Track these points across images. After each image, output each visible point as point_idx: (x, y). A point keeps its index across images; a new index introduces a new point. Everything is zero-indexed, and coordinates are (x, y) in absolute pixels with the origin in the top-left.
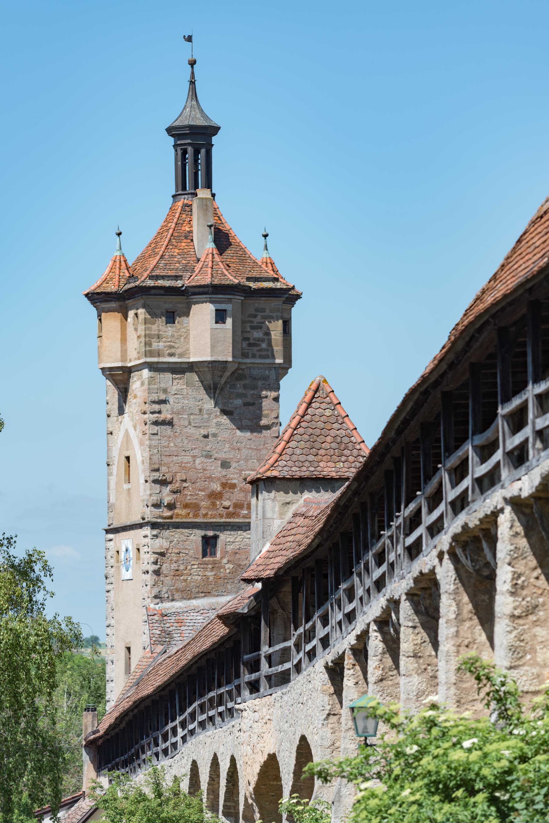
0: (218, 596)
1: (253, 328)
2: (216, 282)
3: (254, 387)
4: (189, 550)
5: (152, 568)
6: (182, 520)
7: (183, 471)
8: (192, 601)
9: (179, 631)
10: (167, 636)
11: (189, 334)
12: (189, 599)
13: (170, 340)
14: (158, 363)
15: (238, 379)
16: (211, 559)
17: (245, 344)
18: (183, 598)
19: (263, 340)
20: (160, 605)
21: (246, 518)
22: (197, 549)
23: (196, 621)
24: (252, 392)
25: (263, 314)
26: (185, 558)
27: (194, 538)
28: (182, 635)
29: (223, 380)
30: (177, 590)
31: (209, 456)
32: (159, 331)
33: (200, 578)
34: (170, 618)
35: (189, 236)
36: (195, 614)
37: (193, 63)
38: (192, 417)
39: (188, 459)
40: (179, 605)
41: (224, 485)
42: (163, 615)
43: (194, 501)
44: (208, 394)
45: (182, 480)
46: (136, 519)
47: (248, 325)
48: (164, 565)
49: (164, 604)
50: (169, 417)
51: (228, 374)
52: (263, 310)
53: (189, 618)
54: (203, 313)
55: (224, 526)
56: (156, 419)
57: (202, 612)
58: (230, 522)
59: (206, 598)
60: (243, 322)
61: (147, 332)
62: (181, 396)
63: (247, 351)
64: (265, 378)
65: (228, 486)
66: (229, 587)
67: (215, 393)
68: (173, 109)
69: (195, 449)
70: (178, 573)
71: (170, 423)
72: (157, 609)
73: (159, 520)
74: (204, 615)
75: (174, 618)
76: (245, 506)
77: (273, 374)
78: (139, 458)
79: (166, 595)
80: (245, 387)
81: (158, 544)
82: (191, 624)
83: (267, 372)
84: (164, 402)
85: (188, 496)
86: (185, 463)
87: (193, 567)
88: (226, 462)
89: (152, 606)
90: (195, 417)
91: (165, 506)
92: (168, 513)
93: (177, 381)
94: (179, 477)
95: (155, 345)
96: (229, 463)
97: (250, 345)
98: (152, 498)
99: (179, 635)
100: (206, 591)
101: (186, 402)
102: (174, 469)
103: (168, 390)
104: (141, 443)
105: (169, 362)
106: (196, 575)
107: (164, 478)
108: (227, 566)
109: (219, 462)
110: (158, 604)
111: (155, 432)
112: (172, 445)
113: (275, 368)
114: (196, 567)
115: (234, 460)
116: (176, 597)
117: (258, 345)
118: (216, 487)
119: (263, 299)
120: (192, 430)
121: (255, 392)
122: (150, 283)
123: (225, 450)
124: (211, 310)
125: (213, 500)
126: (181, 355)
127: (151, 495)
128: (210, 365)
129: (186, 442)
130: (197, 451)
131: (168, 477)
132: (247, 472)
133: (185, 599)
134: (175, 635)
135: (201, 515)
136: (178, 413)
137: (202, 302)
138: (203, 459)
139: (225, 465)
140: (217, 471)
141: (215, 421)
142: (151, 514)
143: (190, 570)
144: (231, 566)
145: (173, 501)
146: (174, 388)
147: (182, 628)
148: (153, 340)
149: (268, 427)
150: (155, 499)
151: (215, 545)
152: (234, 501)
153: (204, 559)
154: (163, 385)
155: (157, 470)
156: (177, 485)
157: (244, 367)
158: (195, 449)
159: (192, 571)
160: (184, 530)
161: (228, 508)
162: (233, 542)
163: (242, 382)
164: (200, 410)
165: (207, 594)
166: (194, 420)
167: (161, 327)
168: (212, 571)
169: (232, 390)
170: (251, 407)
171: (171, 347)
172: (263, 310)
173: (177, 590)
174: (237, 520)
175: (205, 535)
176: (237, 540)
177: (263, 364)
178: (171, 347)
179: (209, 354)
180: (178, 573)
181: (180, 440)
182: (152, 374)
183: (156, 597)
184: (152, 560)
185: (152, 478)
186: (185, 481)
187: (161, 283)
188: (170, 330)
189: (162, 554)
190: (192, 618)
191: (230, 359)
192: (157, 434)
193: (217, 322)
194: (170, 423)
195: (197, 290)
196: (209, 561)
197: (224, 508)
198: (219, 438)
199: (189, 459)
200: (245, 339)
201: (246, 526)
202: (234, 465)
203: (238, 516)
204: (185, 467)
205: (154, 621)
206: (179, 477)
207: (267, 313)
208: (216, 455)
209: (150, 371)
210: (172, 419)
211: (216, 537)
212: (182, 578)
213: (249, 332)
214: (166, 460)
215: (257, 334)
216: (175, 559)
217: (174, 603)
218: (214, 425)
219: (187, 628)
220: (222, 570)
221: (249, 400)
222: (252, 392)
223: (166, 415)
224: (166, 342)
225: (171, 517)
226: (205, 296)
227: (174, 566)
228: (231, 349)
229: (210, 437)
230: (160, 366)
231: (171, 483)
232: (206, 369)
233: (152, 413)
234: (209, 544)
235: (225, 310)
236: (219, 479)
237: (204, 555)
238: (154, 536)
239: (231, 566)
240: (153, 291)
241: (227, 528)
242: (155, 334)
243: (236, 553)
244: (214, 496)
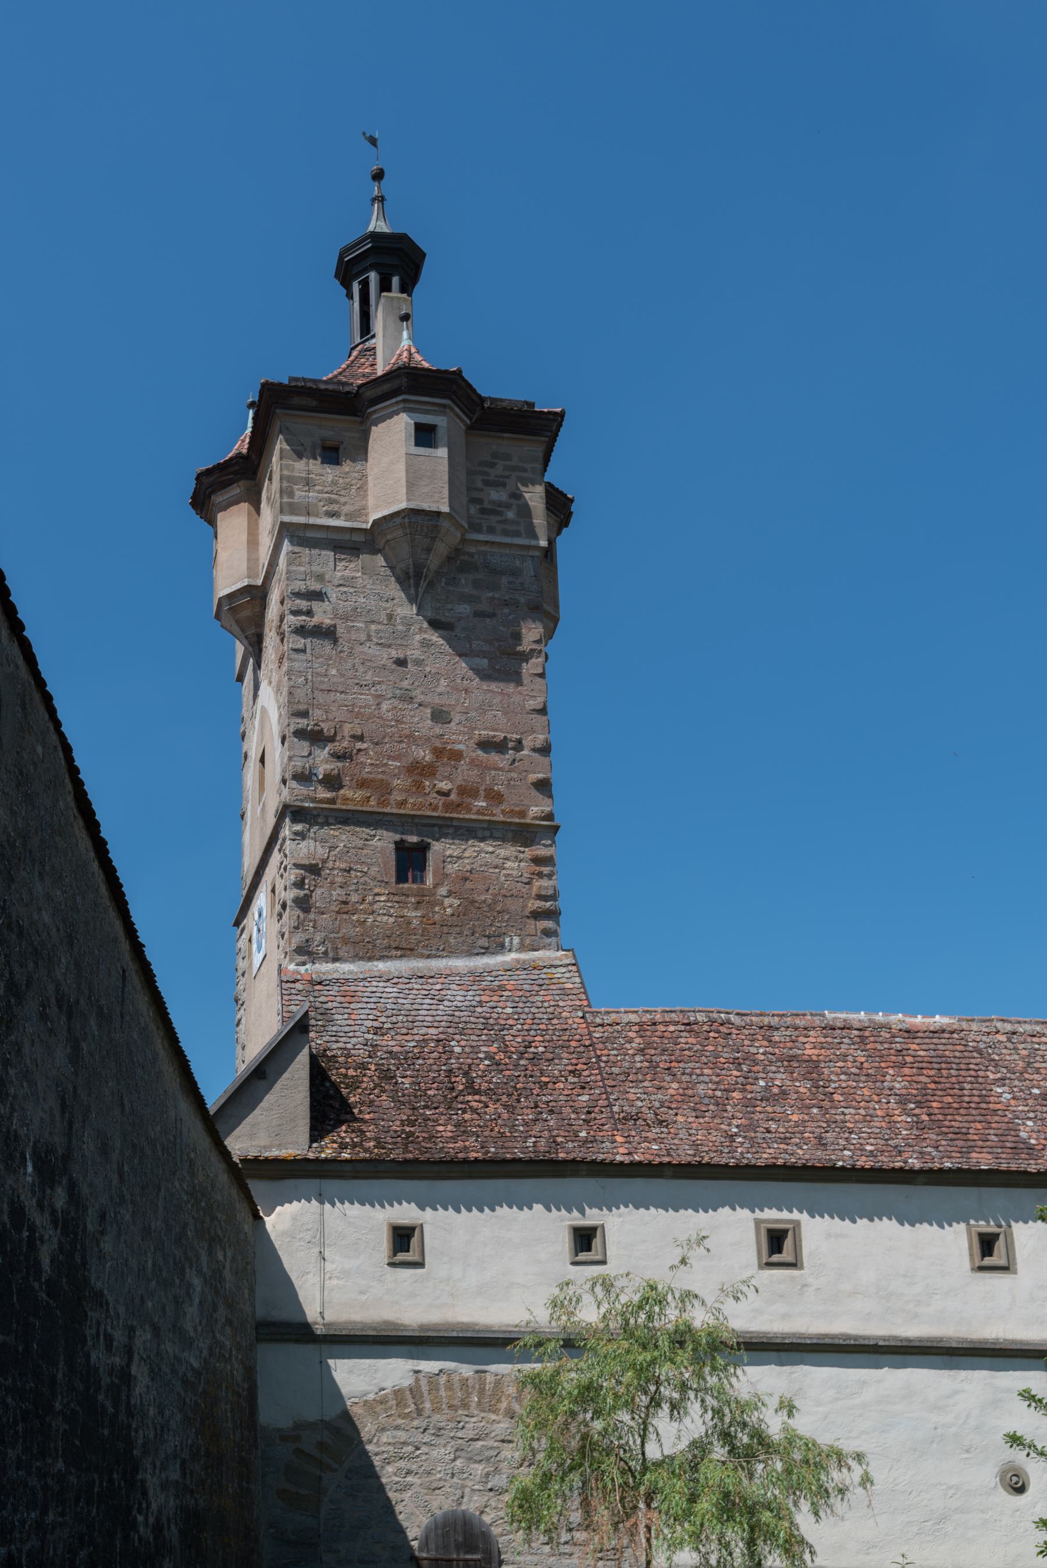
0: (429, 957)
1: (488, 483)
4: (369, 865)
5: (290, 895)
6: (354, 808)
7: (357, 721)
8: (375, 963)
9: (346, 1010)
10: (319, 1017)
11: (366, 483)
12: (370, 959)
13: (329, 489)
14: (306, 526)
16: (415, 886)
17: (473, 510)
18: (357, 957)
19: (508, 506)
20: (308, 966)
21: (483, 814)
22: (385, 864)
23: (384, 995)
24: (491, 595)
25: (507, 463)
26: (362, 880)
27: (379, 843)
28: (353, 1017)
29: (434, 562)
30: (346, 941)
31: (407, 698)
32: (309, 472)
33: (392, 920)
34: (327, 988)
36: (382, 984)
38: (373, 627)
39: (366, 698)
40: (346, 968)
41: (438, 752)
42: (313, 983)
43: (380, 776)
44: (403, 590)
45: (353, 737)
48: (319, 891)
49: (317, 965)
50: (328, 621)
51: (442, 549)
52: (507, 457)
53: (369, 989)
54: (392, 436)
55: (440, 827)
56: (302, 623)
57: (395, 980)
58: (452, 819)
59: (405, 960)
60: (470, 473)
61: (285, 472)
62: (352, 590)
63: (478, 521)
64: (515, 573)
66: (452, 940)
67: (417, 585)
69: (379, 683)
70: (345, 908)
71: (328, 634)
72: (303, 972)
73: (307, 805)
74: (400, 986)
75: (337, 989)
76: (482, 793)
77: (528, 569)
79: (321, 949)
80: (476, 584)
81: (305, 851)
82: (372, 1000)
83: (518, 563)
84: (318, 596)
85: (367, 763)
86: (361, 707)
87: (377, 898)
88: (441, 711)
89: (292, 967)
90: (380, 627)
91: (320, 782)
92: (323, 794)
93: (343, 563)
94: (347, 730)
95: (300, 494)
96: (448, 713)
97: (483, 511)
98: (292, 763)
99: (346, 1016)
100: (405, 946)
102: (340, 714)
103: (327, 577)
105: (328, 527)
106: (384, 911)
107: (316, 728)
108: (447, 902)
109: (429, 711)
110: (304, 964)
111: (300, 646)
112: (334, 672)
113: (532, 557)
114: (383, 898)
115: (458, 709)
116: (341, 954)
117: (500, 513)
118: (425, 755)
119: (506, 435)
120: (371, 650)
121: (497, 596)
123: (439, 690)
124: (407, 423)
125: (417, 778)
126: (350, 517)
127: (290, 758)
128: (406, 520)
129: (361, 669)
130: (384, 687)
131: (327, 728)
132: (482, 732)
133: (361, 959)
134: (336, 1017)
136: (346, 618)
137: (390, 416)
138: (396, 702)
139: (440, 716)
140: (425, 726)
141: (418, 637)
142: (291, 794)
143: (371, 904)
144: (456, 902)
145: (336, 772)
146: (339, 574)
147: (352, 1006)
149: (525, 657)
150: (299, 763)
151: (422, 867)
152: (459, 783)
153: (401, 886)
155: (304, 714)
156: (345, 744)
157: (472, 549)
158: (379, 683)
159: (375, 906)
160: (358, 829)
161: (446, 794)
162: (459, 858)
164: (390, 617)
165: (406, 951)
166: (377, 632)
167: (311, 467)
168: (416, 909)
169: (451, 588)
170: (488, 620)
171: (331, 502)
172: (507, 457)
174: (467, 817)
175: (402, 841)
176: (466, 854)
177: (510, 545)
178: (331, 502)
179: (405, 497)
180: (345, 908)
181: (349, 665)
182: (297, 549)
183: (300, 950)
184: (292, 877)
185: (292, 729)
186: (361, 738)
188: (330, 473)
189: (314, 870)
190: (375, 989)
191: (445, 509)
192: (304, 651)
193: (417, 444)
194: (328, 634)
196: (409, 889)
197: (439, 793)
198: (428, 669)
200: (473, 500)
201: (483, 829)
203: (469, 810)
204: (359, 713)
205: (293, 991)
206: (347, 730)
208: (421, 698)
209: (291, 542)
210: (335, 626)
211: (423, 848)
212: (355, 918)
213: (482, 490)
214: (321, 698)
215: (497, 495)
216: (339, 879)
217: (337, 965)
219: (360, 1005)
220: (437, 909)
222: (491, 595)
223: (323, 615)
224: (319, 492)
225: (332, 801)
226: (394, 400)
227: (337, 893)
228: (446, 492)
229: (409, 666)
230: (310, 534)
231: (332, 739)
232: (399, 533)
233: (295, 613)
234: (410, 861)
236: (428, 740)
237: (401, 878)
238: (296, 833)
239: (456, 902)
240: (296, 401)
241: (446, 831)
242: (302, 478)
243: (466, 879)
244: (419, 771)
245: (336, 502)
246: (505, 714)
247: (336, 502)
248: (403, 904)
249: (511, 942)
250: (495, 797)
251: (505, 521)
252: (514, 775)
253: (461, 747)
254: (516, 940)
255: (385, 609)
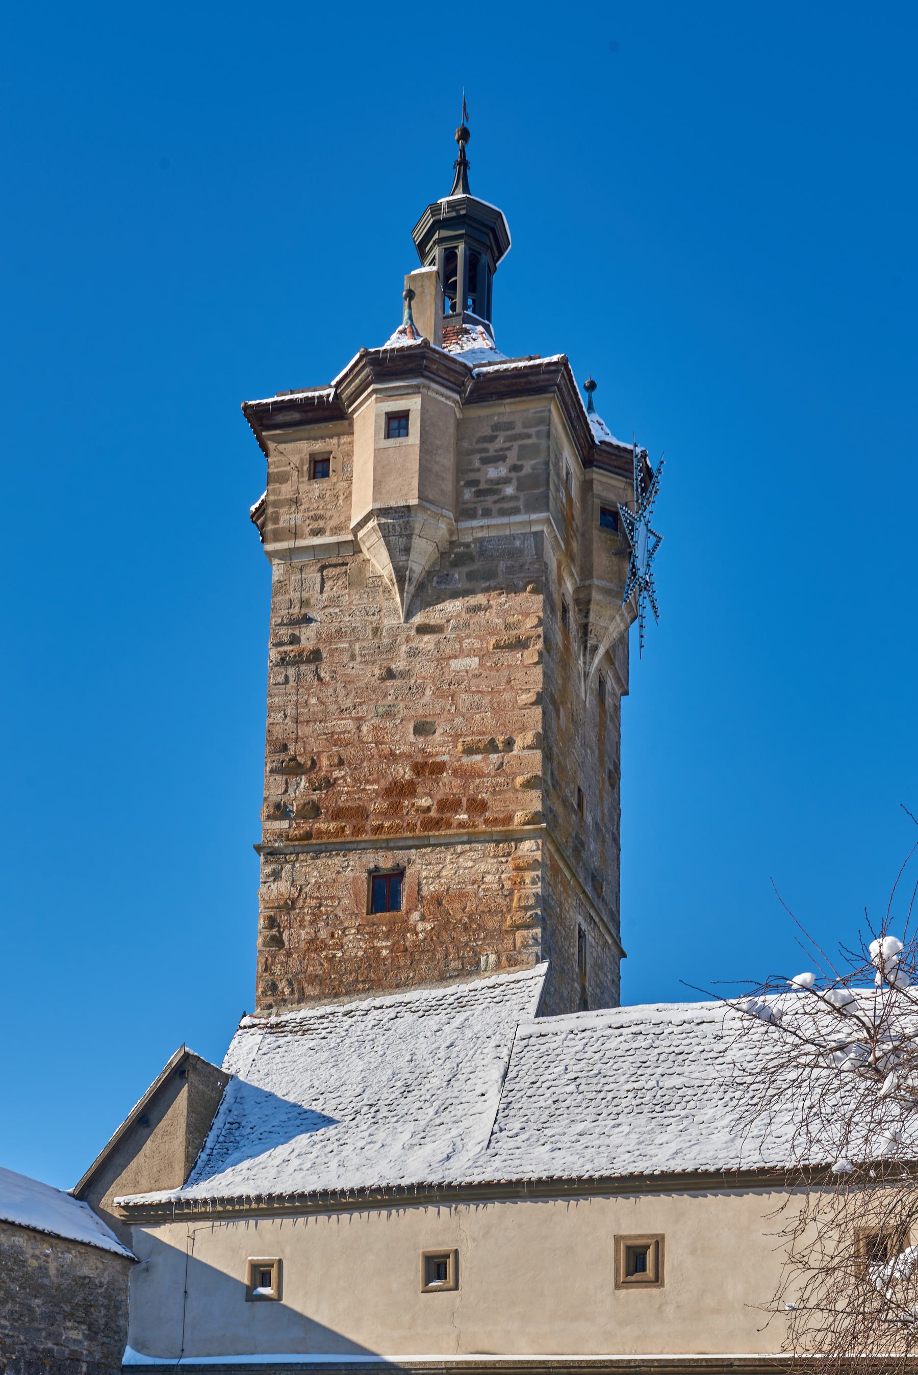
15: (455, 564)
30: (313, 979)
31: (389, 714)
41: (418, 769)
43: (355, 805)
62: (337, 610)
65: (427, 768)
69: (361, 704)
80: (471, 576)
81: (275, 892)
88: (424, 724)
101: (347, 619)
103: (312, 601)
112: (314, 701)
118: (404, 772)
126: (337, 530)
130: (365, 707)
135: (368, 828)
136: (330, 639)
138: (376, 721)
139: (423, 729)
148: (282, 510)
152: (439, 798)
158: (361, 704)
163: (465, 569)
164: (376, 631)
169: (443, 587)
171: (316, 518)
173: (313, 979)
178: (316, 518)
199: (350, 724)
203: (449, 825)
204: (338, 739)
208: (403, 713)
218: (403, 655)
236: (410, 756)
244: (399, 792)
245: (321, 517)
247: (321, 517)
248: (374, 936)
249: (487, 961)
250: (478, 806)
252: (501, 780)
253: (446, 758)
254: (492, 958)
255: (371, 623)
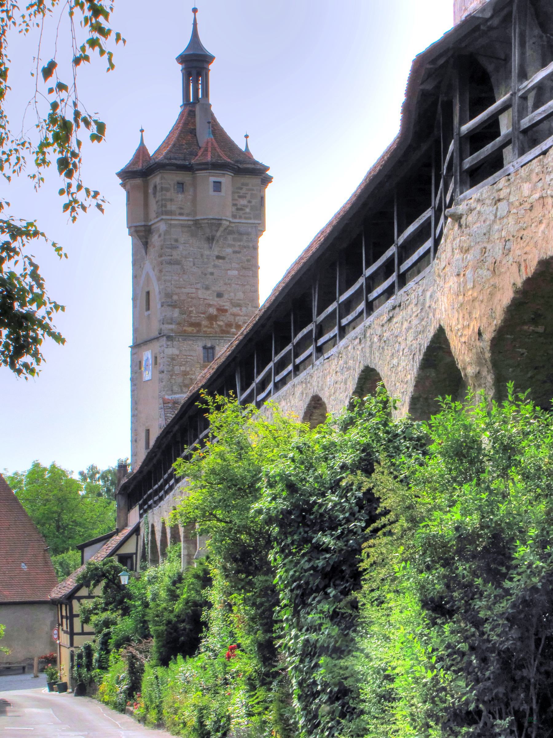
1: (240, 197)
2: (214, 161)
3: (240, 240)
19: (247, 206)
31: (207, 288)
35: (193, 132)
37: (195, 10)
39: (194, 290)
41: (218, 310)
46: (155, 334)
47: (236, 195)
60: (233, 193)
65: (222, 311)
68: (182, 45)
78: (157, 290)
97: (237, 209)
104: (159, 279)
109: (215, 294)
112: (181, 280)
118: (213, 311)
120: (195, 270)
122: (167, 161)
126: (188, 215)
154: (175, 237)
171: (181, 208)
172: (247, 185)
178: (181, 208)
187: (174, 161)
195: (200, 167)
200: (234, 205)
202: (226, 296)
207: (250, 187)
211: (213, 348)
214: (178, 291)
221: (237, 249)
235: (220, 183)
244: (212, 318)
246: (244, 292)
251: (245, 213)
